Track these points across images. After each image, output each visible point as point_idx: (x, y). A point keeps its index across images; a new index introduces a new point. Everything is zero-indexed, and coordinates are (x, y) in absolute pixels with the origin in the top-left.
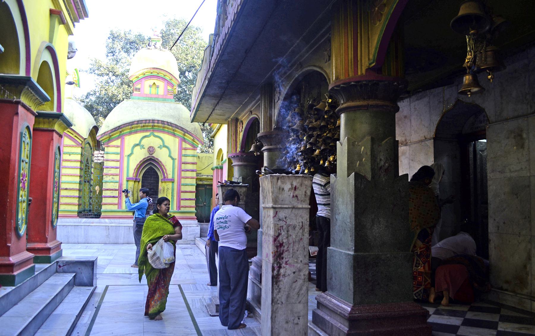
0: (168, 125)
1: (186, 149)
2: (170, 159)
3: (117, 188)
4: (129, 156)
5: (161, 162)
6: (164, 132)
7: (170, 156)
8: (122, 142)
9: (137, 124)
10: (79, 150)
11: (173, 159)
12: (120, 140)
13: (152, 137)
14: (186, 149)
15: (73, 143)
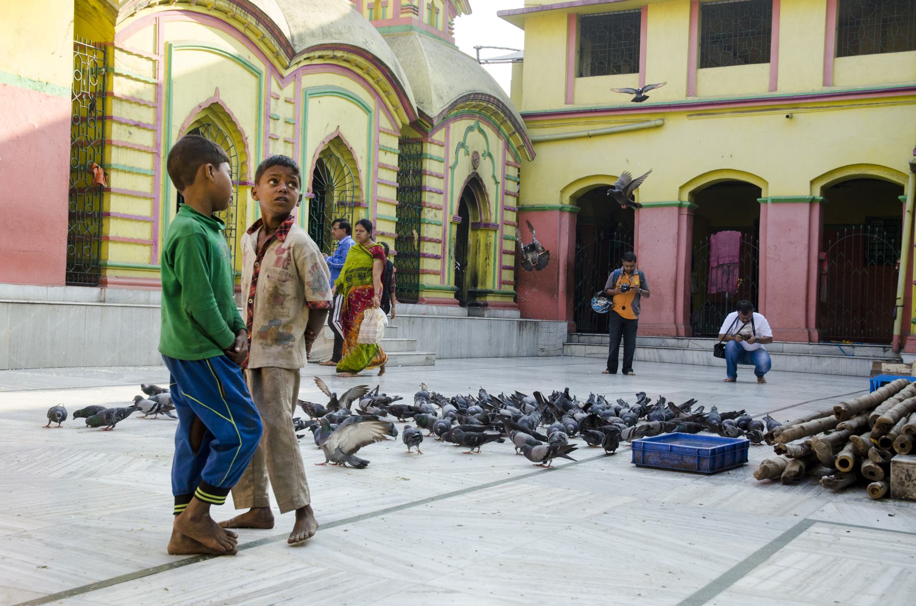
0: (503, 112)
1: (508, 164)
2: (493, 181)
3: (440, 237)
4: (453, 168)
5: (484, 187)
6: (488, 122)
7: (494, 177)
8: (447, 134)
9: (472, 100)
10: (394, 143)
11: (497, 183)
12: (444, 130)
13: (476, 131)
14: (508, 164)
15: (391, 128)
